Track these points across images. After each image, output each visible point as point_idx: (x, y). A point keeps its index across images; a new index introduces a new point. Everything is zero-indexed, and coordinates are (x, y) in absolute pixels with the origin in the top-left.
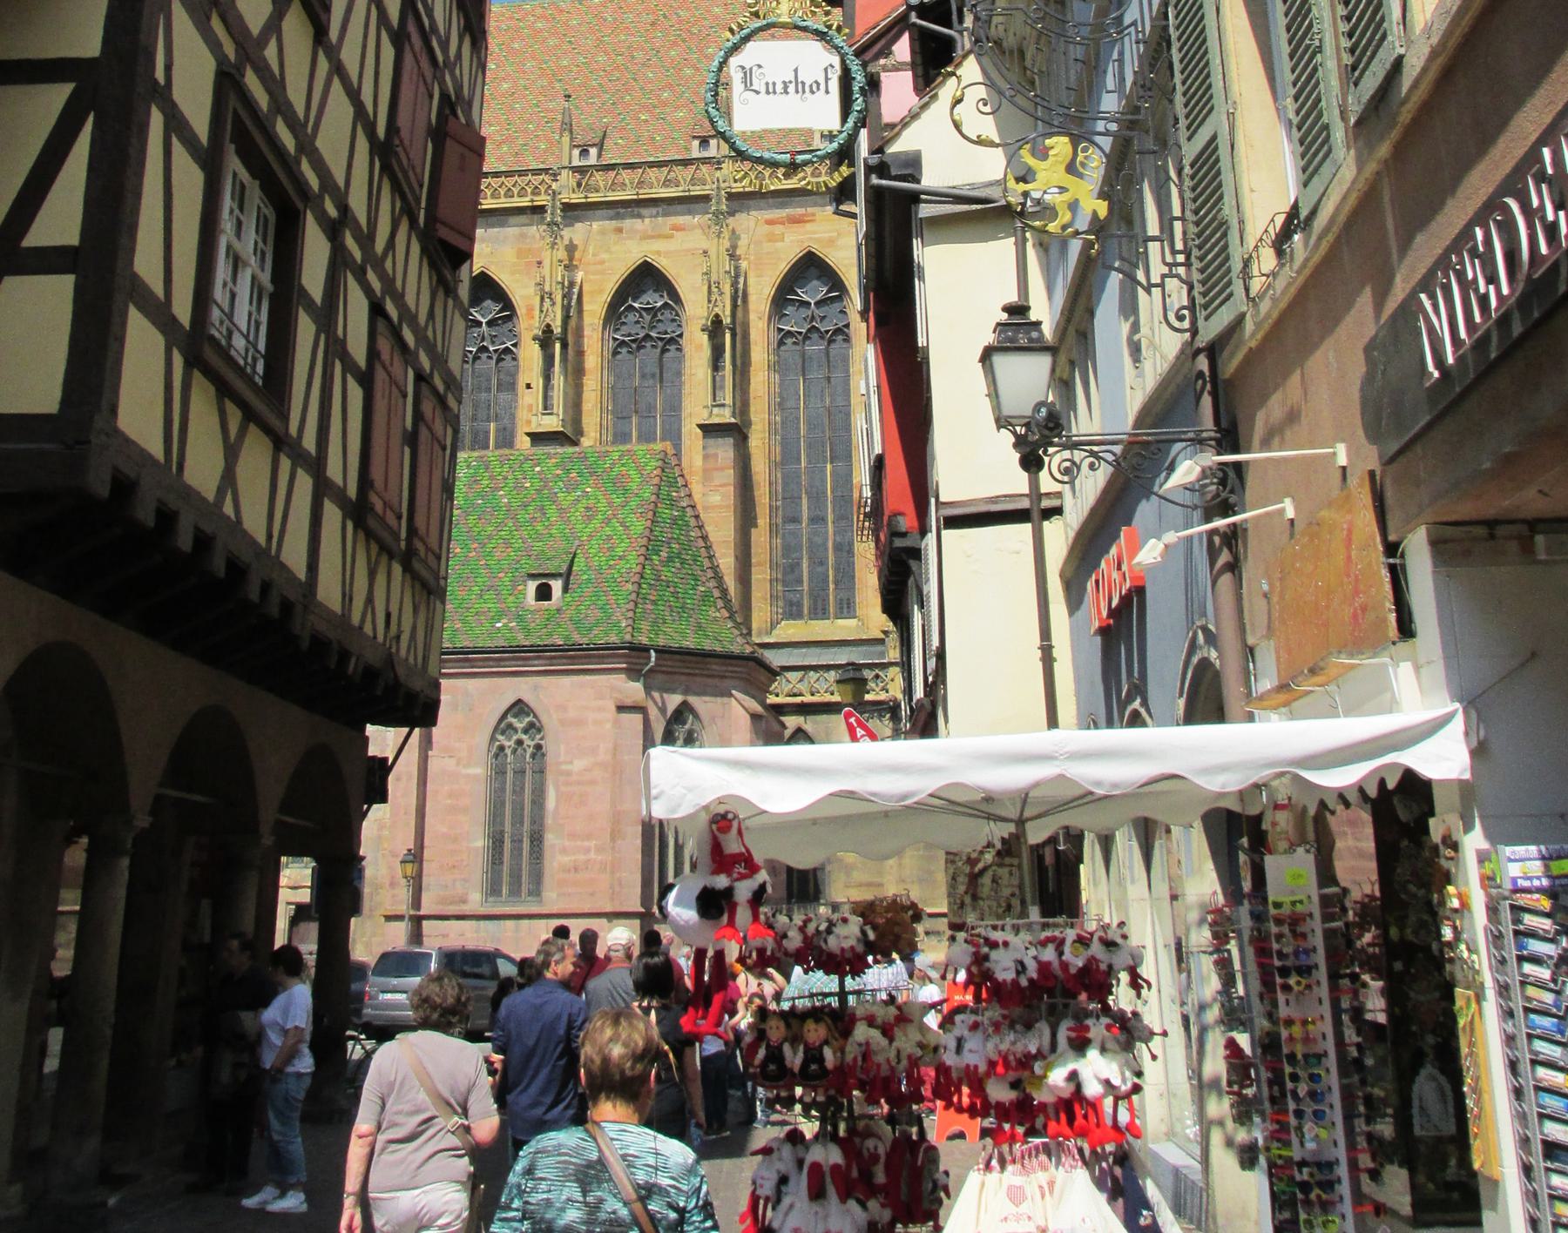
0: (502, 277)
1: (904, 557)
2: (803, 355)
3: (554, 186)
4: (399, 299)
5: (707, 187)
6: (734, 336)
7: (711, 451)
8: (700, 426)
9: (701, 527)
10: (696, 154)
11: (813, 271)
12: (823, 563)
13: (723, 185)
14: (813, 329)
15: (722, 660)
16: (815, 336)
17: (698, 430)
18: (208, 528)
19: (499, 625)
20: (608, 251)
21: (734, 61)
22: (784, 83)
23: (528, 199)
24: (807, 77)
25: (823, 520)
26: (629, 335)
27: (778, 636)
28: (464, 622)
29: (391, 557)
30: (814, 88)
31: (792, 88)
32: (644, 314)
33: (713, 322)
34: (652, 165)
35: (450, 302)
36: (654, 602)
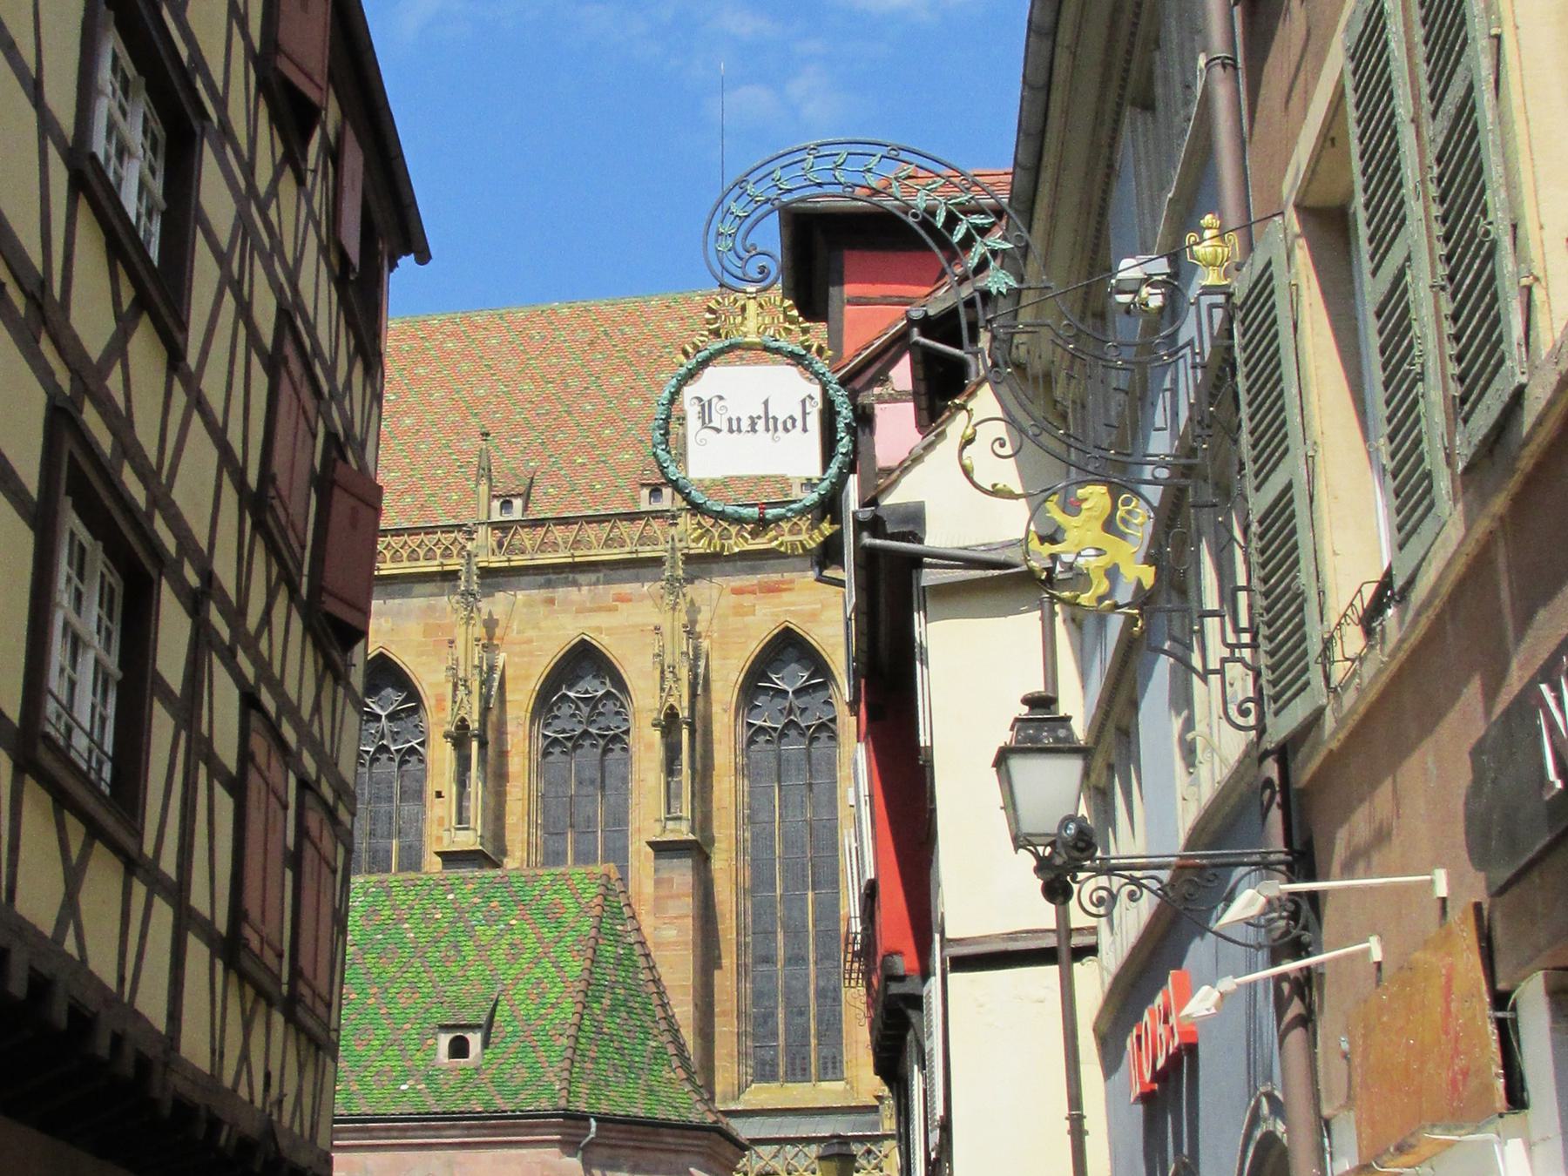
0: (405, 659)
1: (902, 1005)
3: (469, 546)
4: (277, 687)
5: (660, 547)
10: (645, 506)
11: (791, 652)
12: (802, 1013)
13: (679, 545)
15: (677, 1132)
16: (793, 733)
17: (649, 850)
18: (45, 969)
19: (404, 1087)
20: (537, 627)
21: (689, 392)
22: (751, 418)
23: (436, 563)
24: (780, 411)
25: (804, 960)
26: (564, 731)
27: (746, 1102)
28: (361, 1081)
29: (270, 1004)
30: (789, 425)
31: (761, 425)
32: (581, 705)
33: (666, 715)
34: (590, 520)
35: (341, 691)
36: (594, 1060)
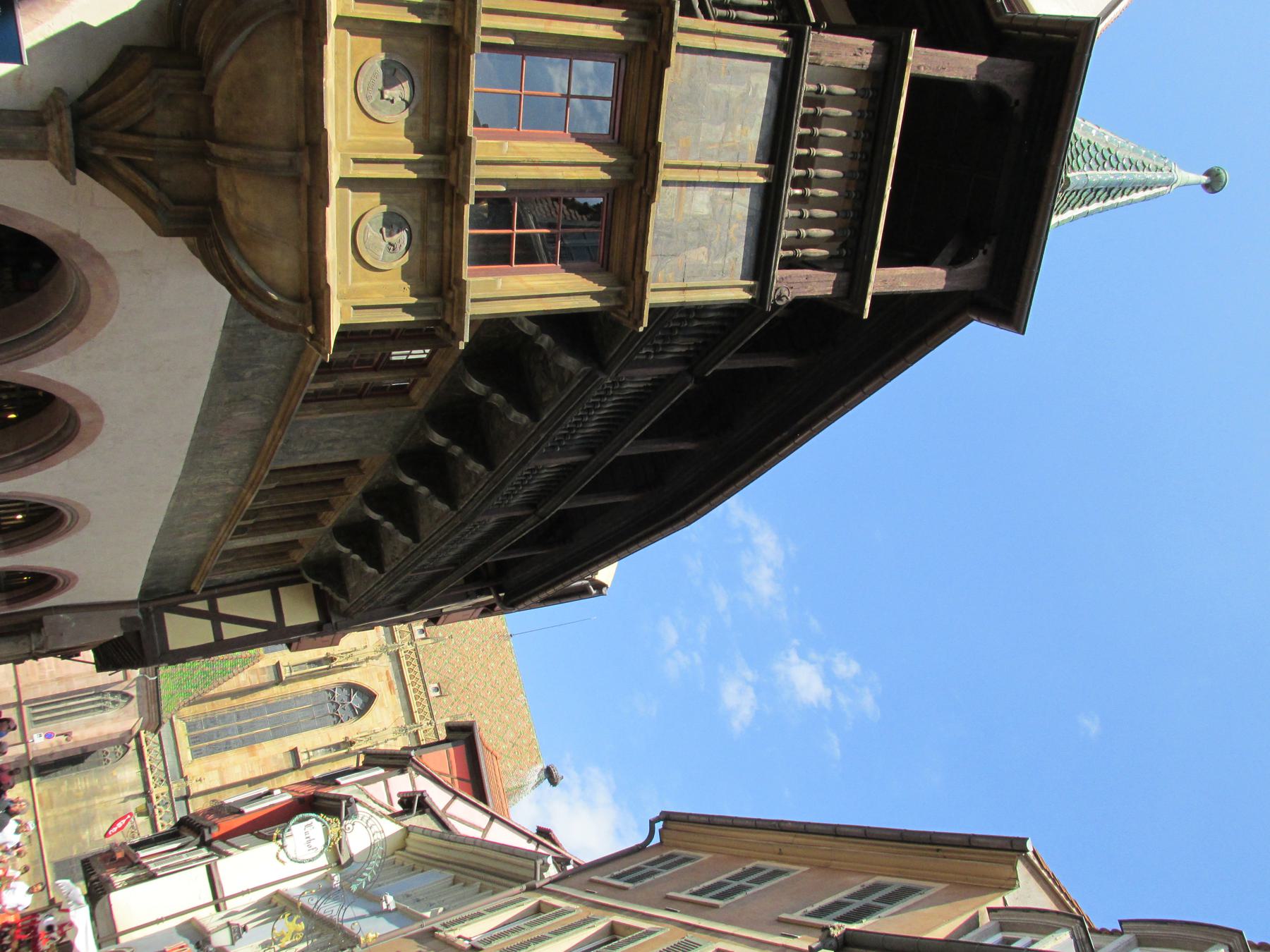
2: (324, 703)
6: (327, 669)
7: (267, 670)
8: (278, 663)
9: (224, 681)
11: (367, 699)
14: (338, 706)
16: (334, 707)
